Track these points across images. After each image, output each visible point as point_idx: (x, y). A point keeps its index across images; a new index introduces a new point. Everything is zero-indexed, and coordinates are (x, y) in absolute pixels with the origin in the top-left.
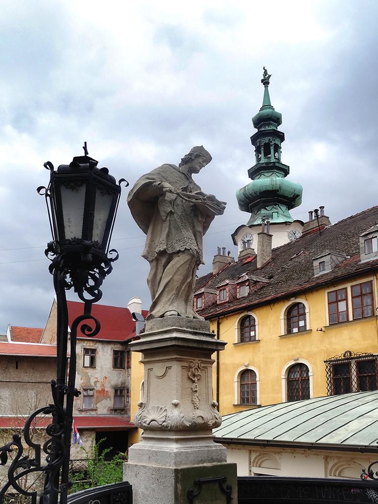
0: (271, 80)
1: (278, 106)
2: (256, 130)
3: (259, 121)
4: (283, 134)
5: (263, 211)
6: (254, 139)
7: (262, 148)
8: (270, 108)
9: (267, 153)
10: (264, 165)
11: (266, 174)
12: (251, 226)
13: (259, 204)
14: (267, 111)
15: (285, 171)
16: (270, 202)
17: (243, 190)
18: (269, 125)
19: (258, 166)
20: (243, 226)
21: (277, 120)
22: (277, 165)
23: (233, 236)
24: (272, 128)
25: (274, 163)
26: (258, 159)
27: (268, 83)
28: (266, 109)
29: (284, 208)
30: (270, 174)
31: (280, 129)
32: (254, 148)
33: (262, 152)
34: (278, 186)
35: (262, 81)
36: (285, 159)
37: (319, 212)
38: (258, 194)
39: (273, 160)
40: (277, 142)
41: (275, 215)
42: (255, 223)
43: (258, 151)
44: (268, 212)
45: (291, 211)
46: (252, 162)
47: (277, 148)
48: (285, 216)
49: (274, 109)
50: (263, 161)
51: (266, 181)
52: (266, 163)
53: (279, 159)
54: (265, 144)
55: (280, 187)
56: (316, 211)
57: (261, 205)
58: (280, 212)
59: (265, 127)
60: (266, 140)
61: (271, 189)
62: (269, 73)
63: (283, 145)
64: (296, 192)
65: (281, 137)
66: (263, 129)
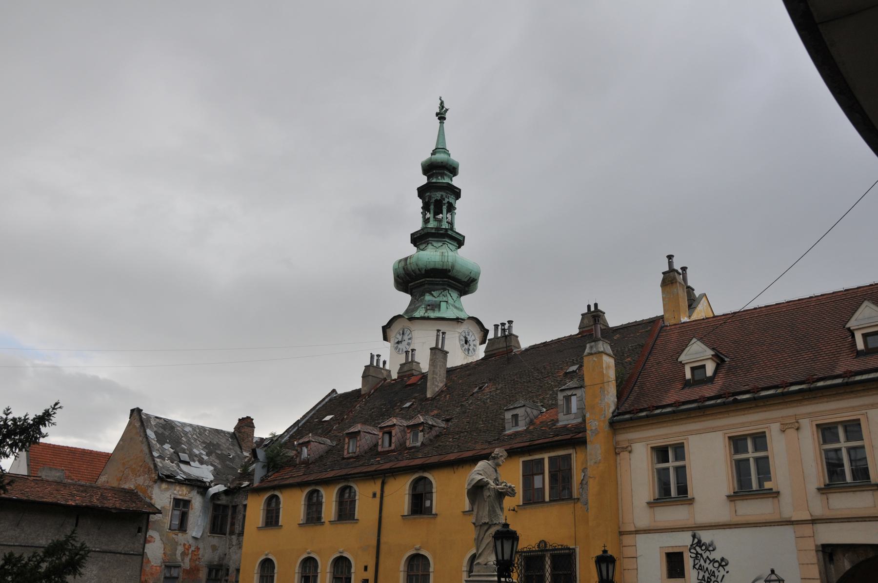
0: (447, 115)
1: (455, 156)
2: (423, 180)
3: (430, 168)
4: (460, 190)
5: (428, 297)
6: (422, 192)
7: (432, 207)
8: (445, 152)
9: (438, 211)
10: (433, 231)
11: (435, 244)
12: (411, 319)
13: (424, 285)
14: (440, 157)
15: (459, 241)
16: (437, 284)
17: (403, 263)
18: (443, 175)
19: (426, 231)
20: (399, 316)
21: (453, 170)
22: (450, 232)
23: (385, 329)
24: (446, 180)
25: (446, 230)
26: (426, 221)
27: (445, 119)
28: (440, 152)
29: (455, 295)
30: (440, 244)
31: (456, 182)
32: (419, 203)
33: (432, 211)
34: (450, 264)
35: (437, 114)
36: (458, 228)
37: (506, 327)
38: (423, 272)
39: (445, 225)
40: (452, 200)
41: (443, 305)
42: (417, 314)
43: (426, 208)
44: (434, 299)
45: (464, 298)
46: (417, 225)
47: (451, 208)
48: (456, 307)
49: (449, 155)
50: (432, 224)
51: (434, 255)
52: (437, 229)
53: (451, 224)
54: (436, 200)
55: (453, 267)
56: (503, 324)
57: (426, 286)
58: (450, 301)
59: (437, 178)
60: (438, 195)
61: (439, 266)
62: (446, 106)
63: (458, 204)
64: (472, 275)
65: (457, 193)
66: (434, 180)
